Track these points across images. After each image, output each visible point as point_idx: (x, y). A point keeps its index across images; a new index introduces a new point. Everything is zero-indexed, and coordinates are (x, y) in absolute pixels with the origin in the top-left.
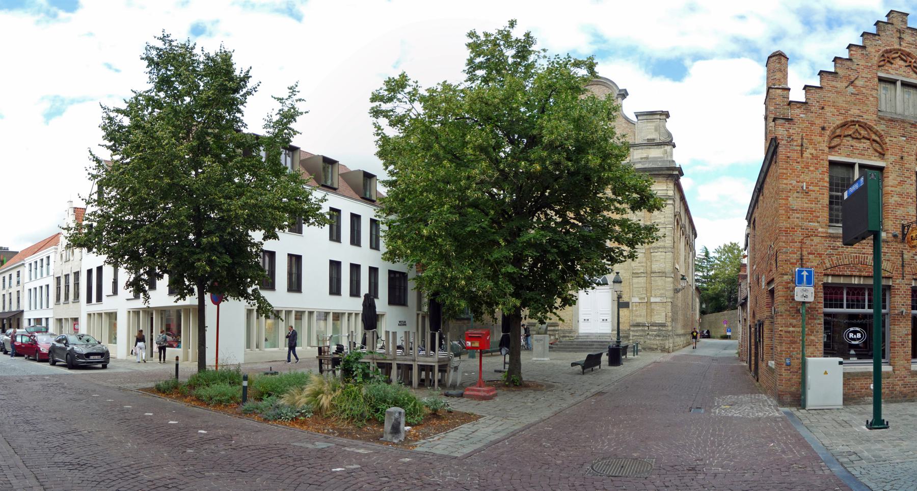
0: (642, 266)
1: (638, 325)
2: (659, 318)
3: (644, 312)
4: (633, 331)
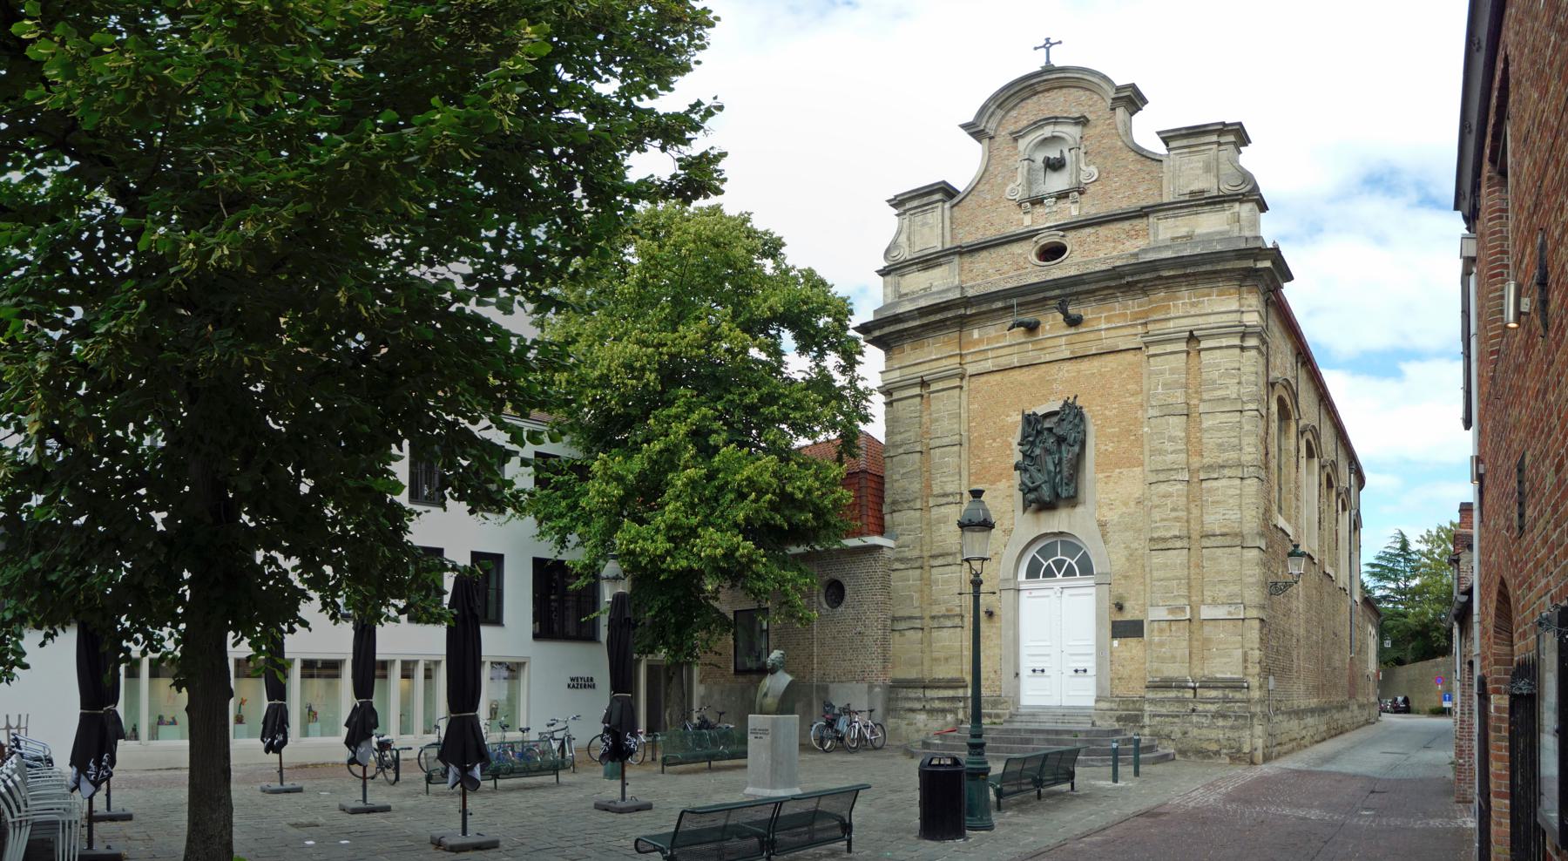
0: (1177, 519)
1: (1165, 685)
2: (1226, 666)
3: (1182, 648)
4: (1152, 702)
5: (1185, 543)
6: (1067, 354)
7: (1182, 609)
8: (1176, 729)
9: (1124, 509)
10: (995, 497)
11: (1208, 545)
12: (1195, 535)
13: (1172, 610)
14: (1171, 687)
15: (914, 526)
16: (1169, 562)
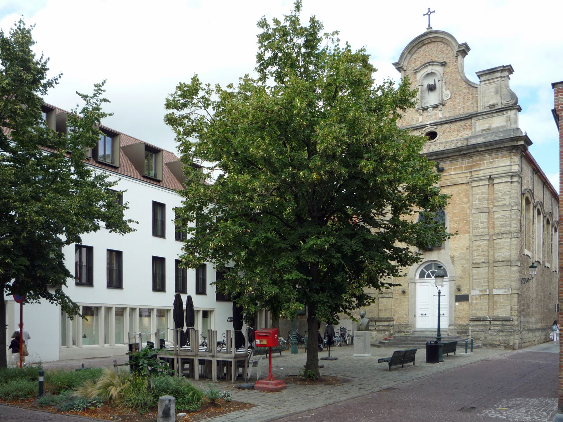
0: (484, 255)
1: (478, 319)
2: (503, 311)
3: (485, 306)
4: (472, 326)
5: (487, 265)
7: (485, 290)
8: (482, 336)
9: (461, 251)
12: (491, 261)
14: (480, 320)
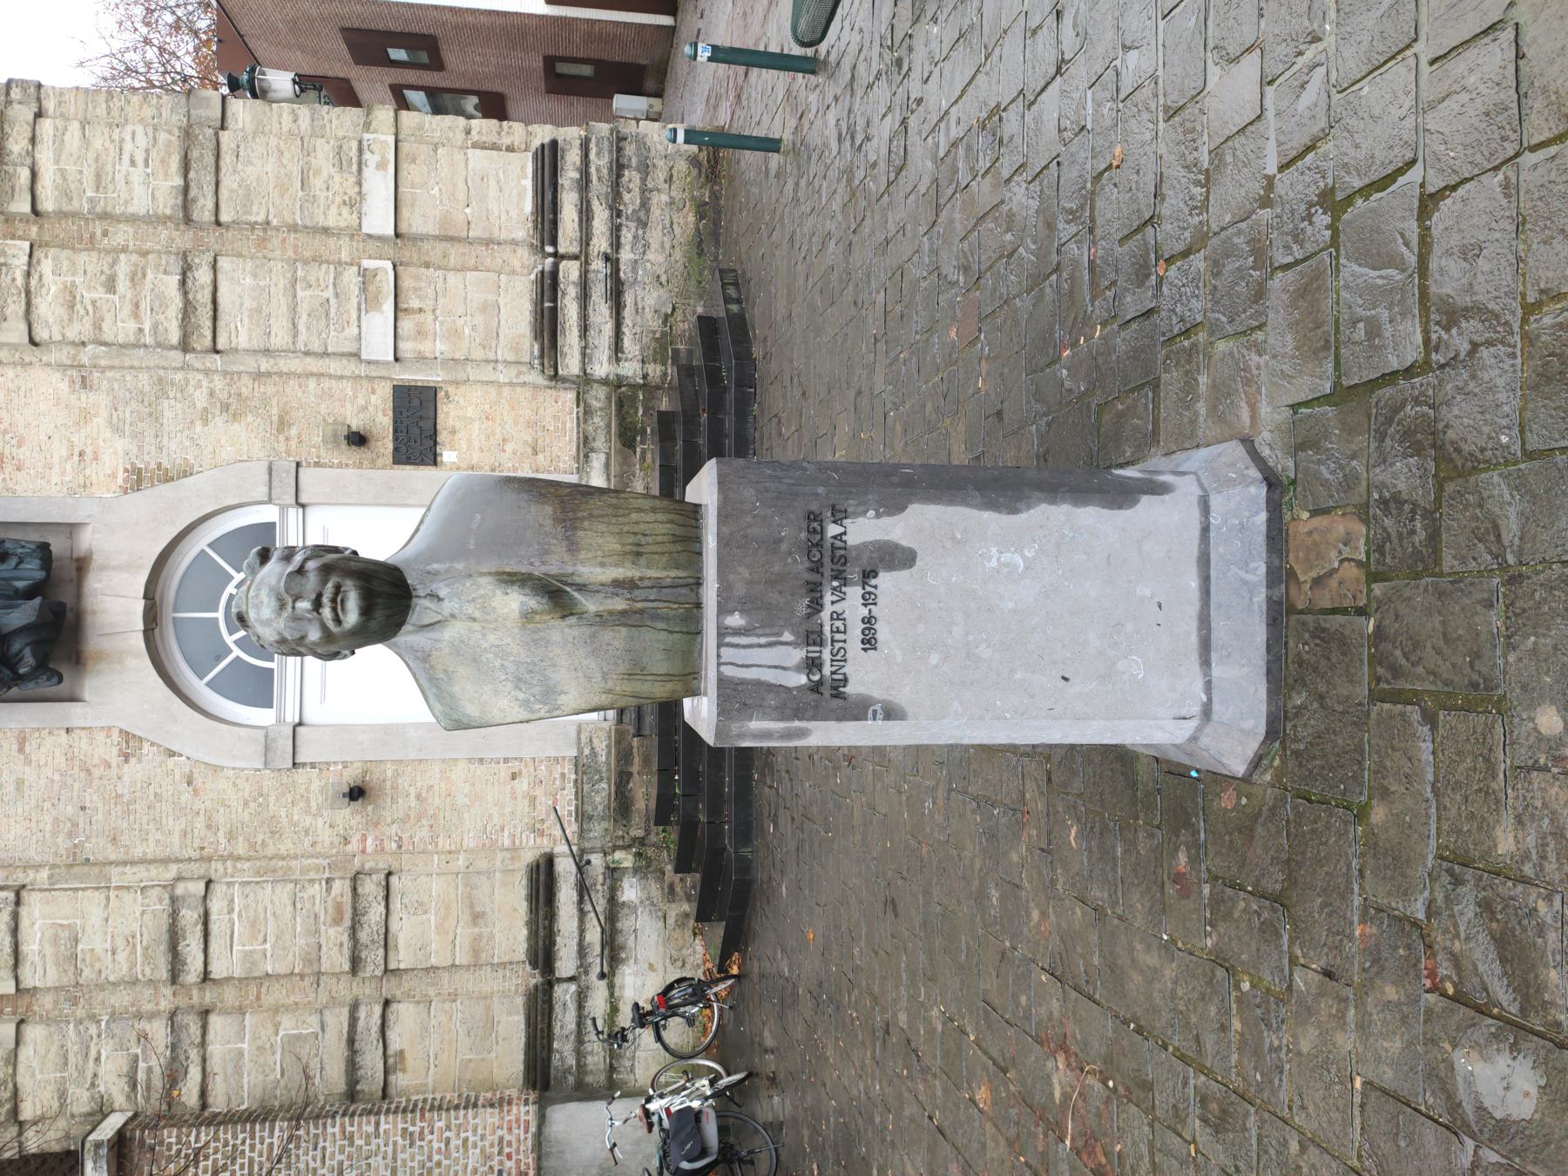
0: (136, 278)
1: (547, 326)
6: (381, 951)
9: (100, 421)
10: (20, 784)
11: (210, 204)
13: (368, 299)
14: (554, 310)
15: (73, 1049)
16: (248, 304)
